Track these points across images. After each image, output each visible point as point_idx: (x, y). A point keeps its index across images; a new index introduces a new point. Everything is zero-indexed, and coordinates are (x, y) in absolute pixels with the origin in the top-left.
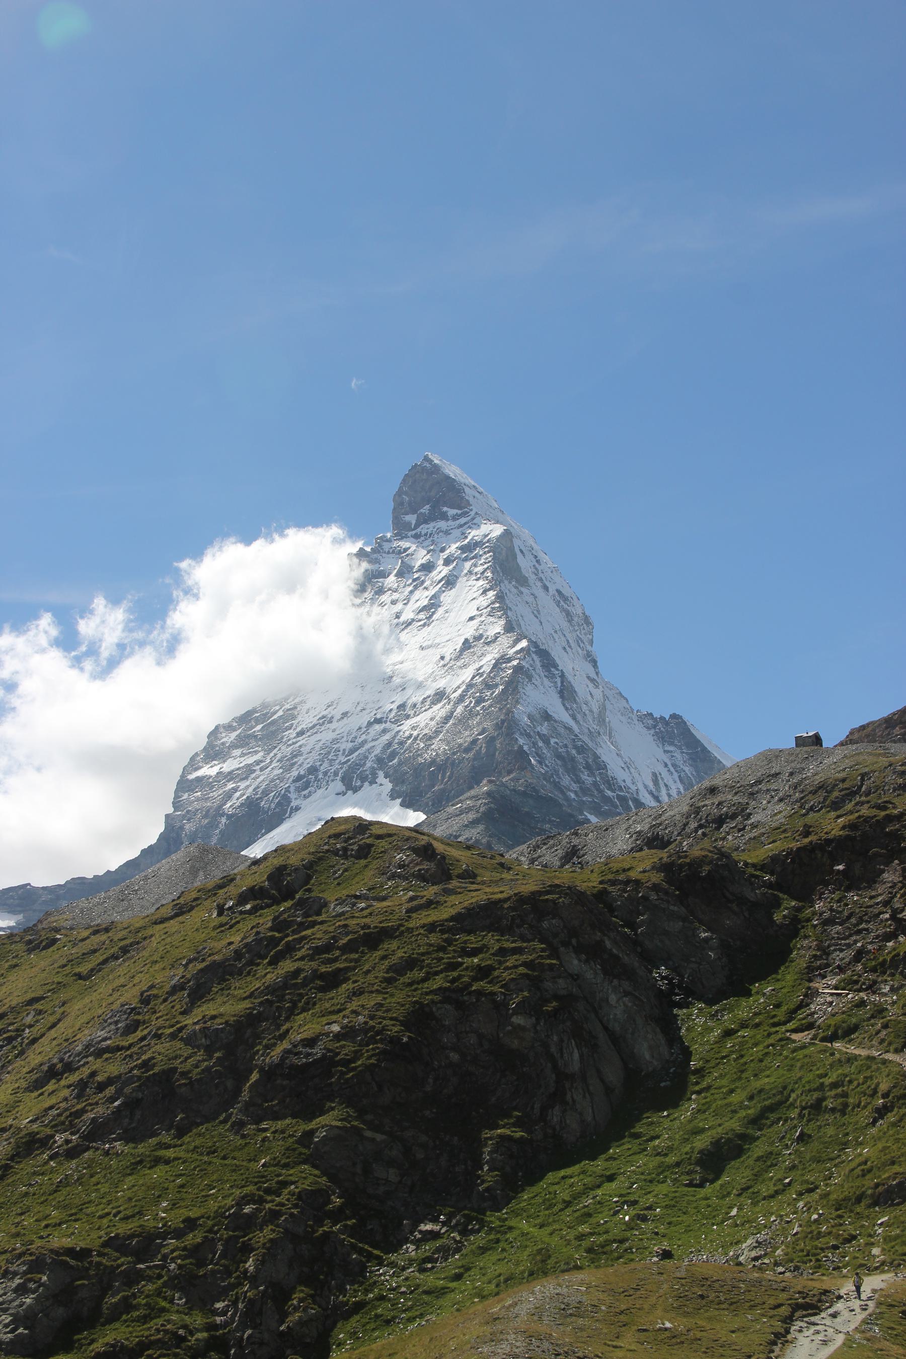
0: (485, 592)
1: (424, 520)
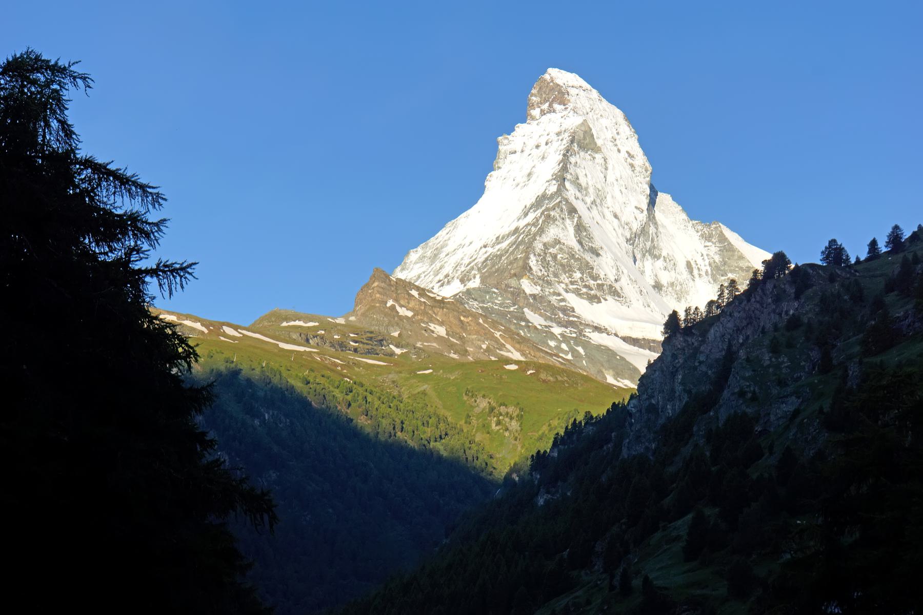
1: (543, 113)
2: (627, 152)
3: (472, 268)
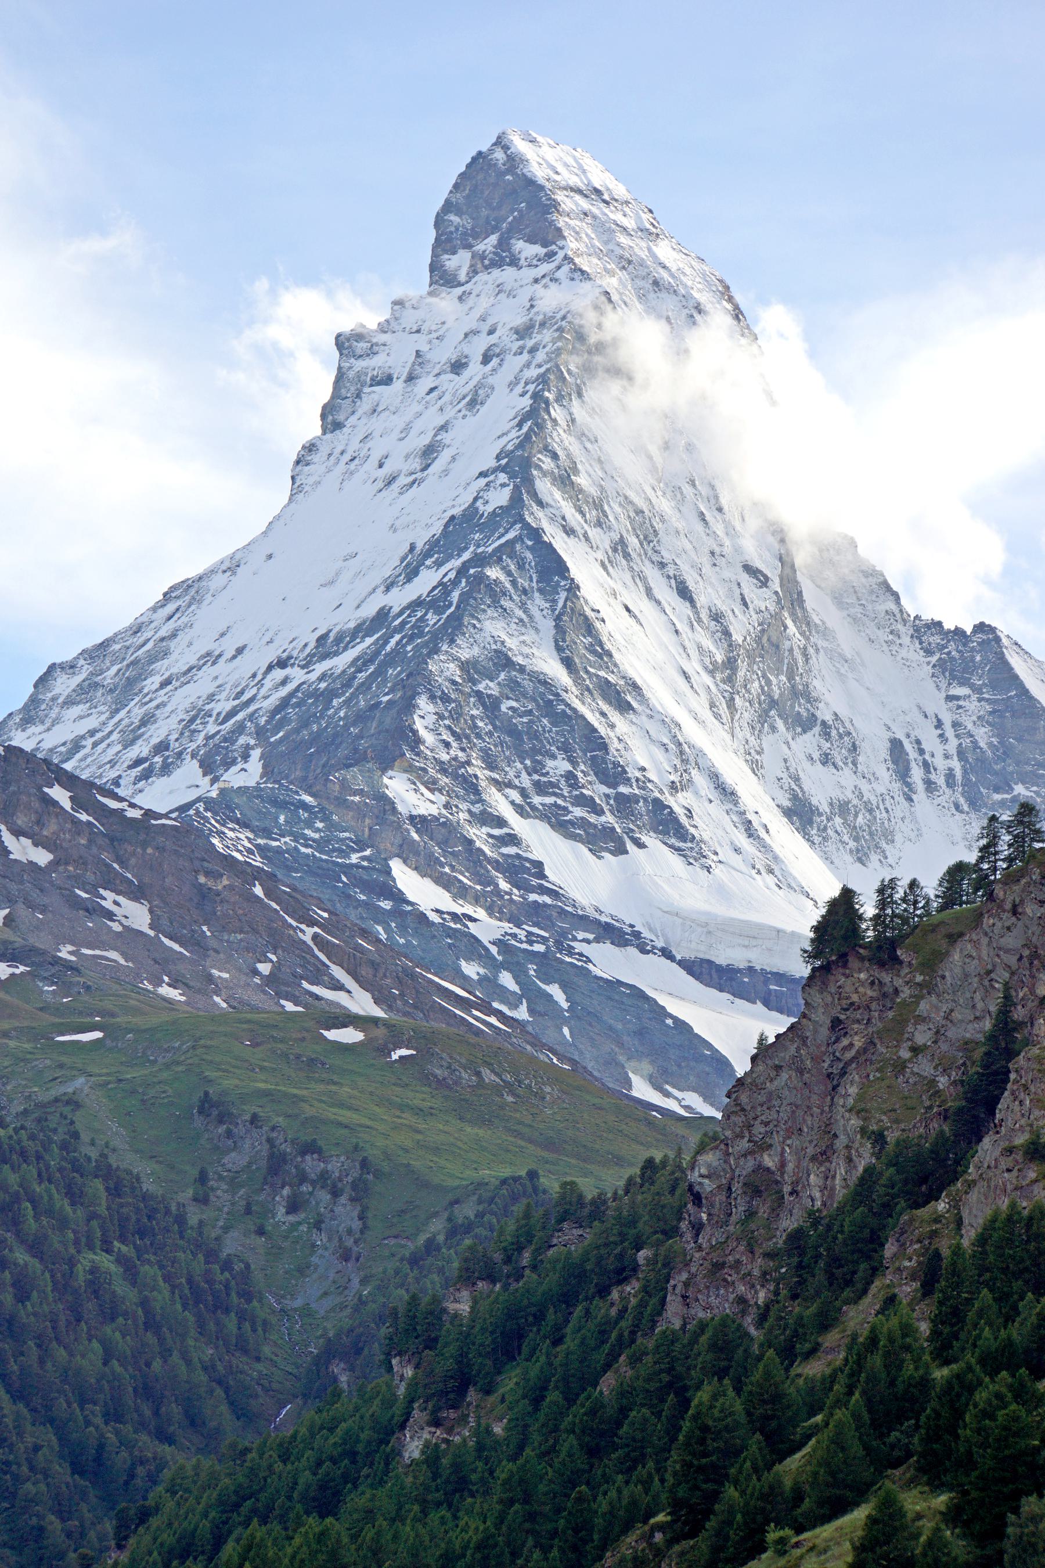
0: (520, 425)
3: (240, 728)
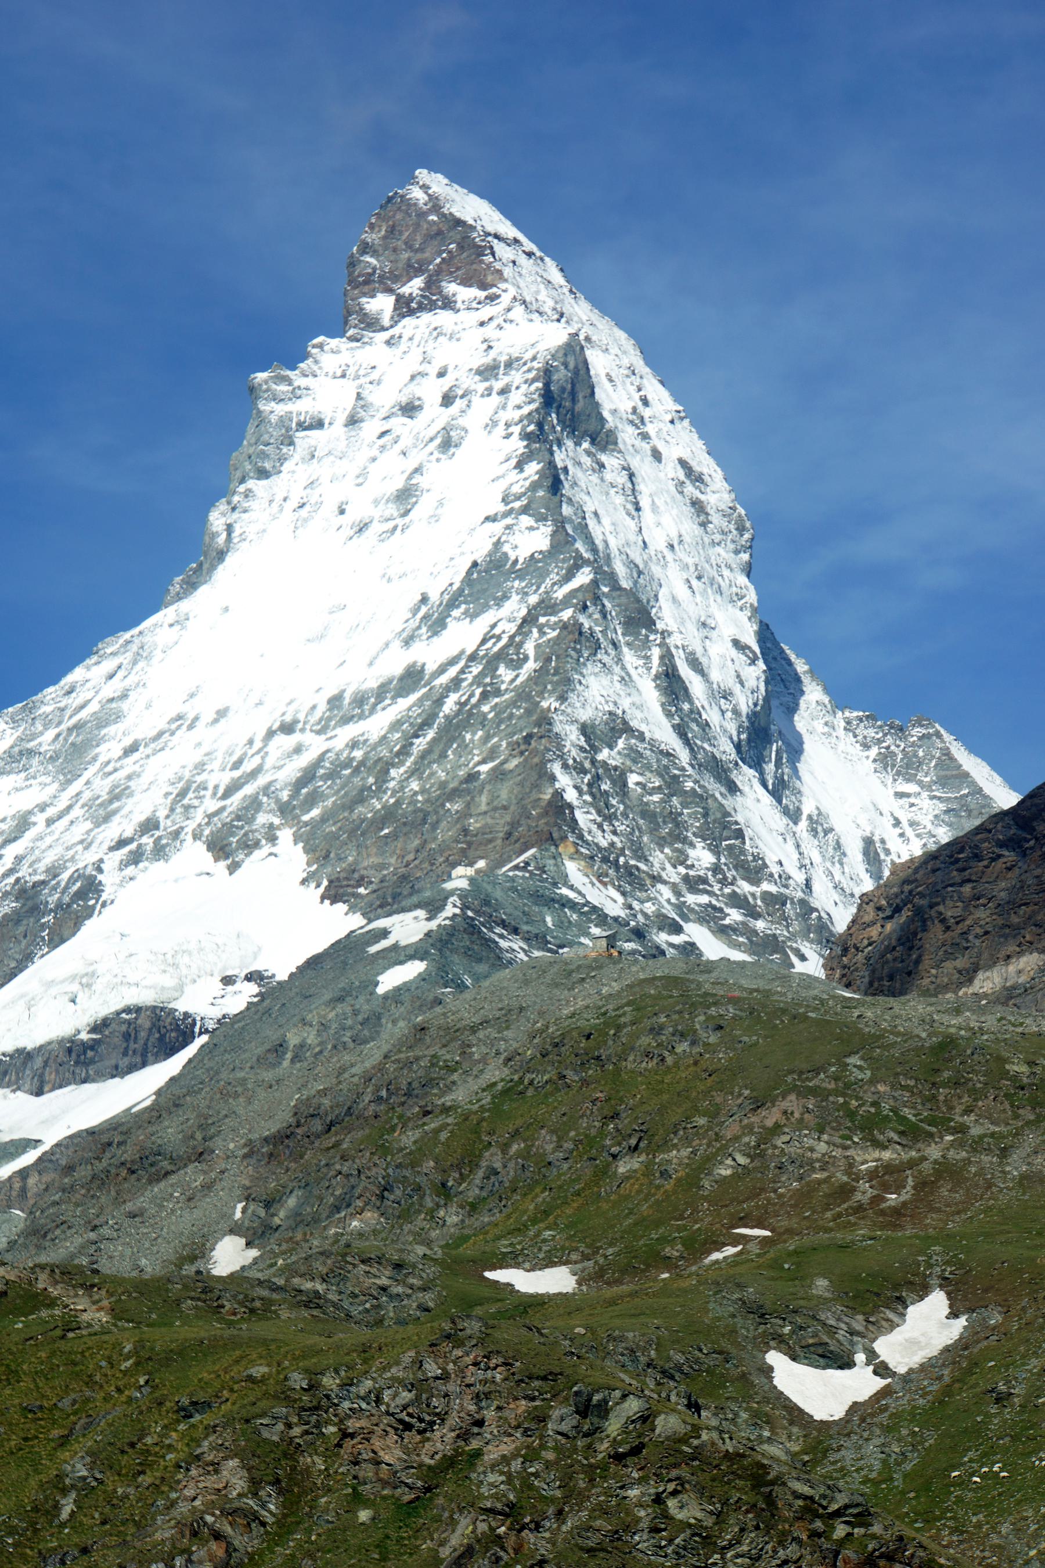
0: (520, 466)
2: (683, 463)
3: (253, 805)
